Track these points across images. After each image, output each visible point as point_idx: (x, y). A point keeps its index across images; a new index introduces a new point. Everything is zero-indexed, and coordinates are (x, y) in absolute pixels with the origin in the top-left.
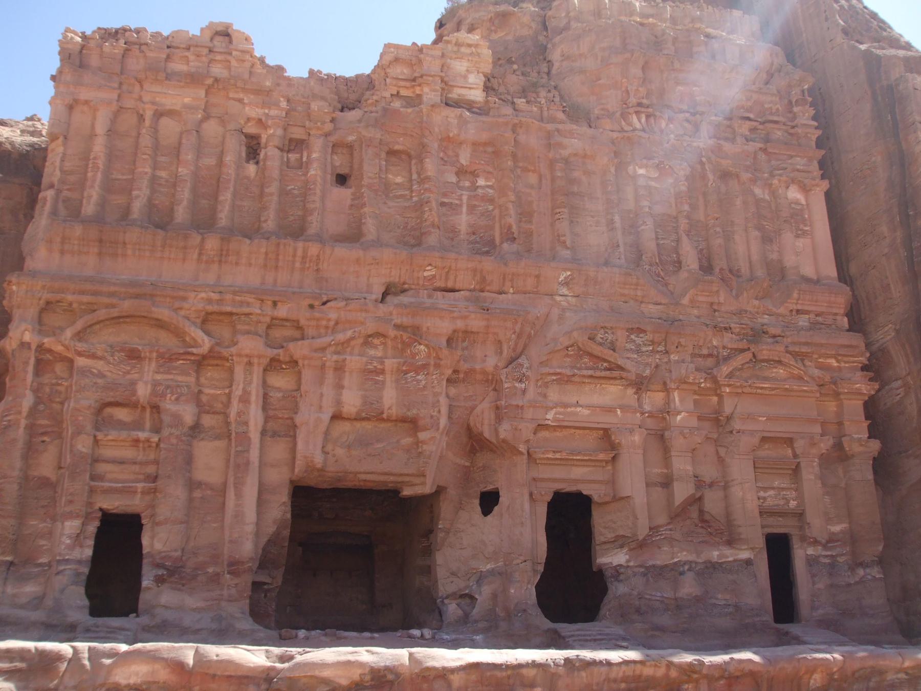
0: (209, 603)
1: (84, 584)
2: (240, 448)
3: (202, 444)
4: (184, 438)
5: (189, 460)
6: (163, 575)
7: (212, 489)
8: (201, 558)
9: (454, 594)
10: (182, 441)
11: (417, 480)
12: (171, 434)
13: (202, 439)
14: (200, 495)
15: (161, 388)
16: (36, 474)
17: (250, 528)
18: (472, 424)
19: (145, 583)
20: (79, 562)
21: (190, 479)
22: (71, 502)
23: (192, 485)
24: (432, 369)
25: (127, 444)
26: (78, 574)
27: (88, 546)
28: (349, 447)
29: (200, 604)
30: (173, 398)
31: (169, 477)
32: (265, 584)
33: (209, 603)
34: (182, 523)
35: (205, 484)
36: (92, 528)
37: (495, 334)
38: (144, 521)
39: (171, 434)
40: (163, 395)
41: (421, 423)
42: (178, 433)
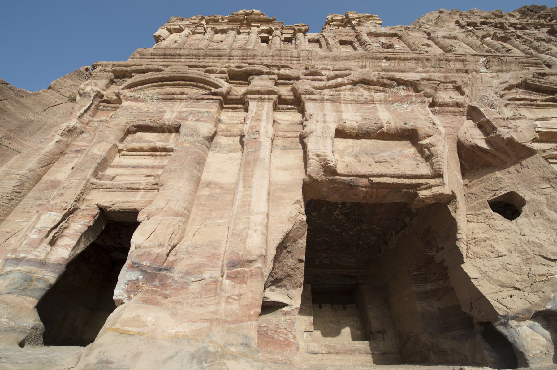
0: (197, 326)
1: (40, 294)
2: (250, 150)
3: (217, 155)
4: (197, 144)
5: (201, 163)
6: (137, 280)
7: (221, 188)
8: (197, 260)
9: (528, 311)
10: (194, 145)
11: (432, 182)
12: (185, 141)
13: (218, 152)
14: (208, 193)
15: (184, 115)
16: (51, 178)
17: (258, 219)
18: (462, 140)
19: (118, 293)
20: (42, 264)
21: (199, 179)
22: (61, 195)
23: (197, 182)
24: (414, 99)
25: (146, 153)
26: (29, 279)
27: (66, 246)
28: (356, 157)
29: (184, 328)
30: (194, 119)
31: (175, 171)
32: (285, 305)
33: (197, 326)
34: (177, 214)
35: (215, 184)
36: (79, 225)
37: (452, 82)
38: (140, 218)
39: (185, 141)
40: (186, 119)
41: (421, 132)
42: (194, 140)
